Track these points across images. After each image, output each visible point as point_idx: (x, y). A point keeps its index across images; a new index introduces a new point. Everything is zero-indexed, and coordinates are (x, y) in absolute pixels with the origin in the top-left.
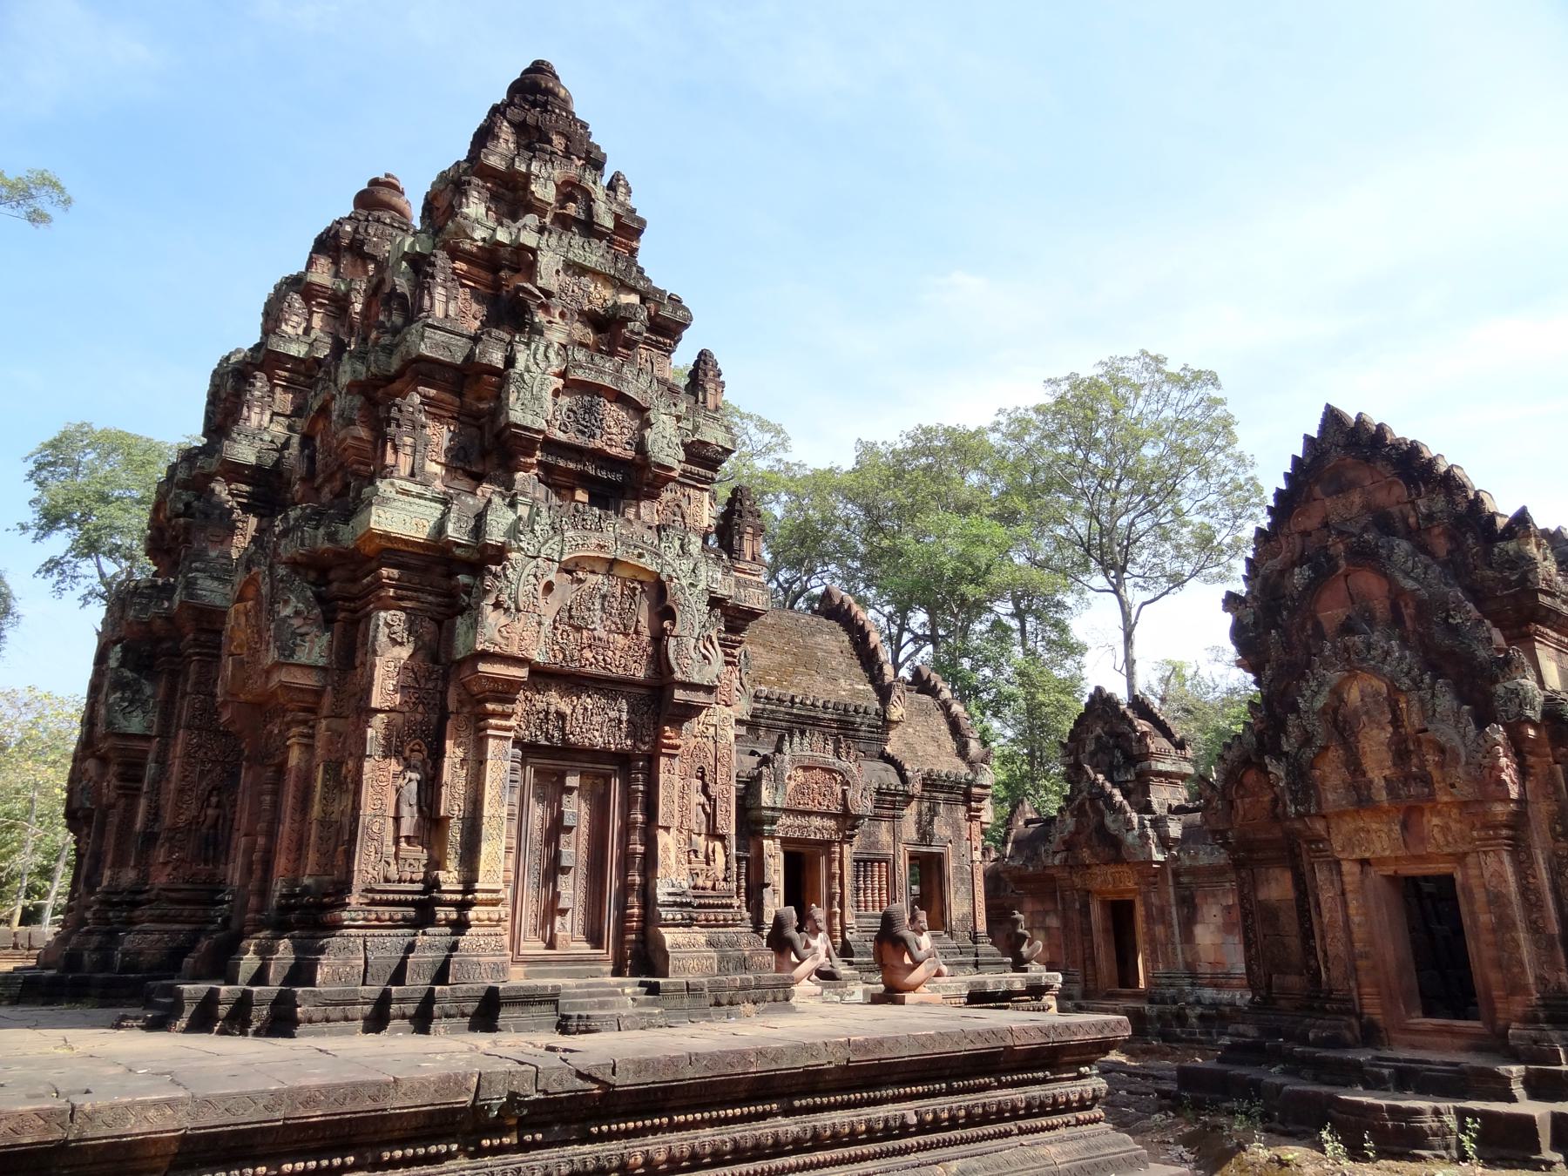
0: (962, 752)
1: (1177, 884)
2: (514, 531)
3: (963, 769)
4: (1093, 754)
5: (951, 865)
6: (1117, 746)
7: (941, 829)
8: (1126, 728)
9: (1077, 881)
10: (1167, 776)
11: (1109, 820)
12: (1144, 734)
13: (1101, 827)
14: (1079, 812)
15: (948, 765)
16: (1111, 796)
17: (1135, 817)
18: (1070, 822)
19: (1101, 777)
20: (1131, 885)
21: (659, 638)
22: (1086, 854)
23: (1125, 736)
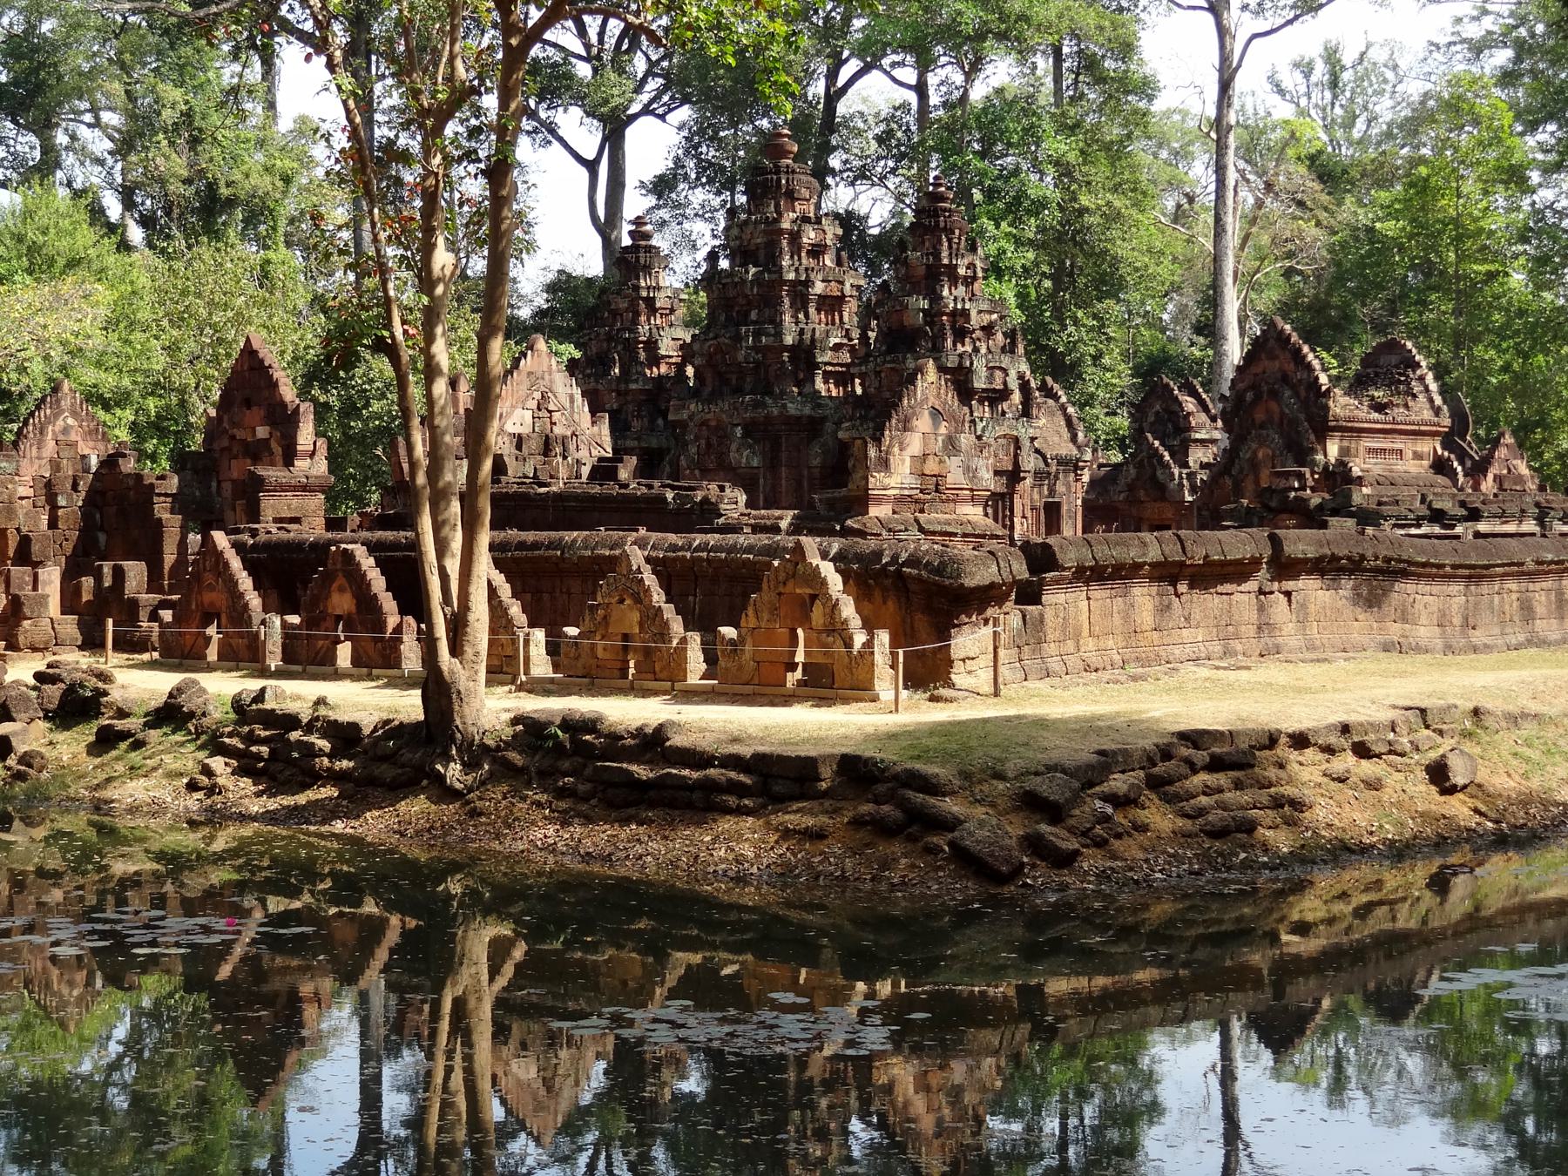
0: (1074, 439)
1: (1199, 514)
2: (983, 430)
3: (1075, 452)
4: (1152, 424)
5: (1065, 508)
6: (1169, 420)
7: (1060, 488)
8: (1176, 408)
9: (1134, 512)
10: (1202, 442)
11: (1159, 473)
12: (1189, 414)
13: (1154, 476)
14: (1140, 466)
15: (1067, 450)
16: (1162, 456)
17: (1176, 471)
18: (1133, 471)
19: (1157, 443)
20: (1170, 515)
21: (1016, 456)
22: (1142, 493)
23: (1175, 414)
